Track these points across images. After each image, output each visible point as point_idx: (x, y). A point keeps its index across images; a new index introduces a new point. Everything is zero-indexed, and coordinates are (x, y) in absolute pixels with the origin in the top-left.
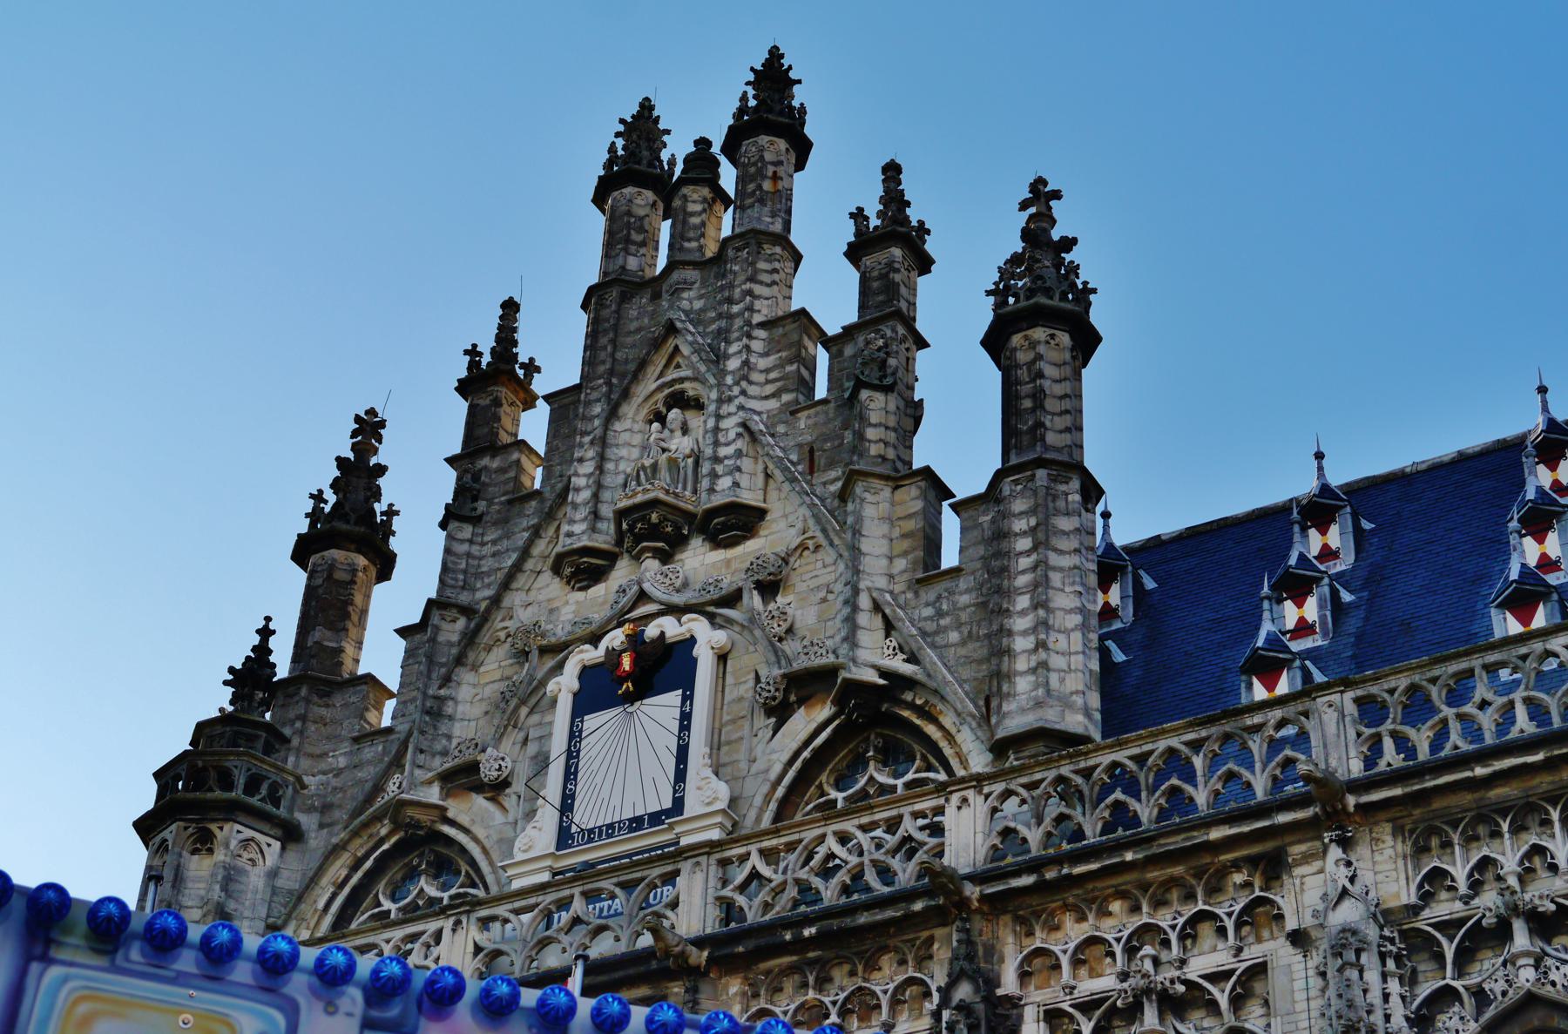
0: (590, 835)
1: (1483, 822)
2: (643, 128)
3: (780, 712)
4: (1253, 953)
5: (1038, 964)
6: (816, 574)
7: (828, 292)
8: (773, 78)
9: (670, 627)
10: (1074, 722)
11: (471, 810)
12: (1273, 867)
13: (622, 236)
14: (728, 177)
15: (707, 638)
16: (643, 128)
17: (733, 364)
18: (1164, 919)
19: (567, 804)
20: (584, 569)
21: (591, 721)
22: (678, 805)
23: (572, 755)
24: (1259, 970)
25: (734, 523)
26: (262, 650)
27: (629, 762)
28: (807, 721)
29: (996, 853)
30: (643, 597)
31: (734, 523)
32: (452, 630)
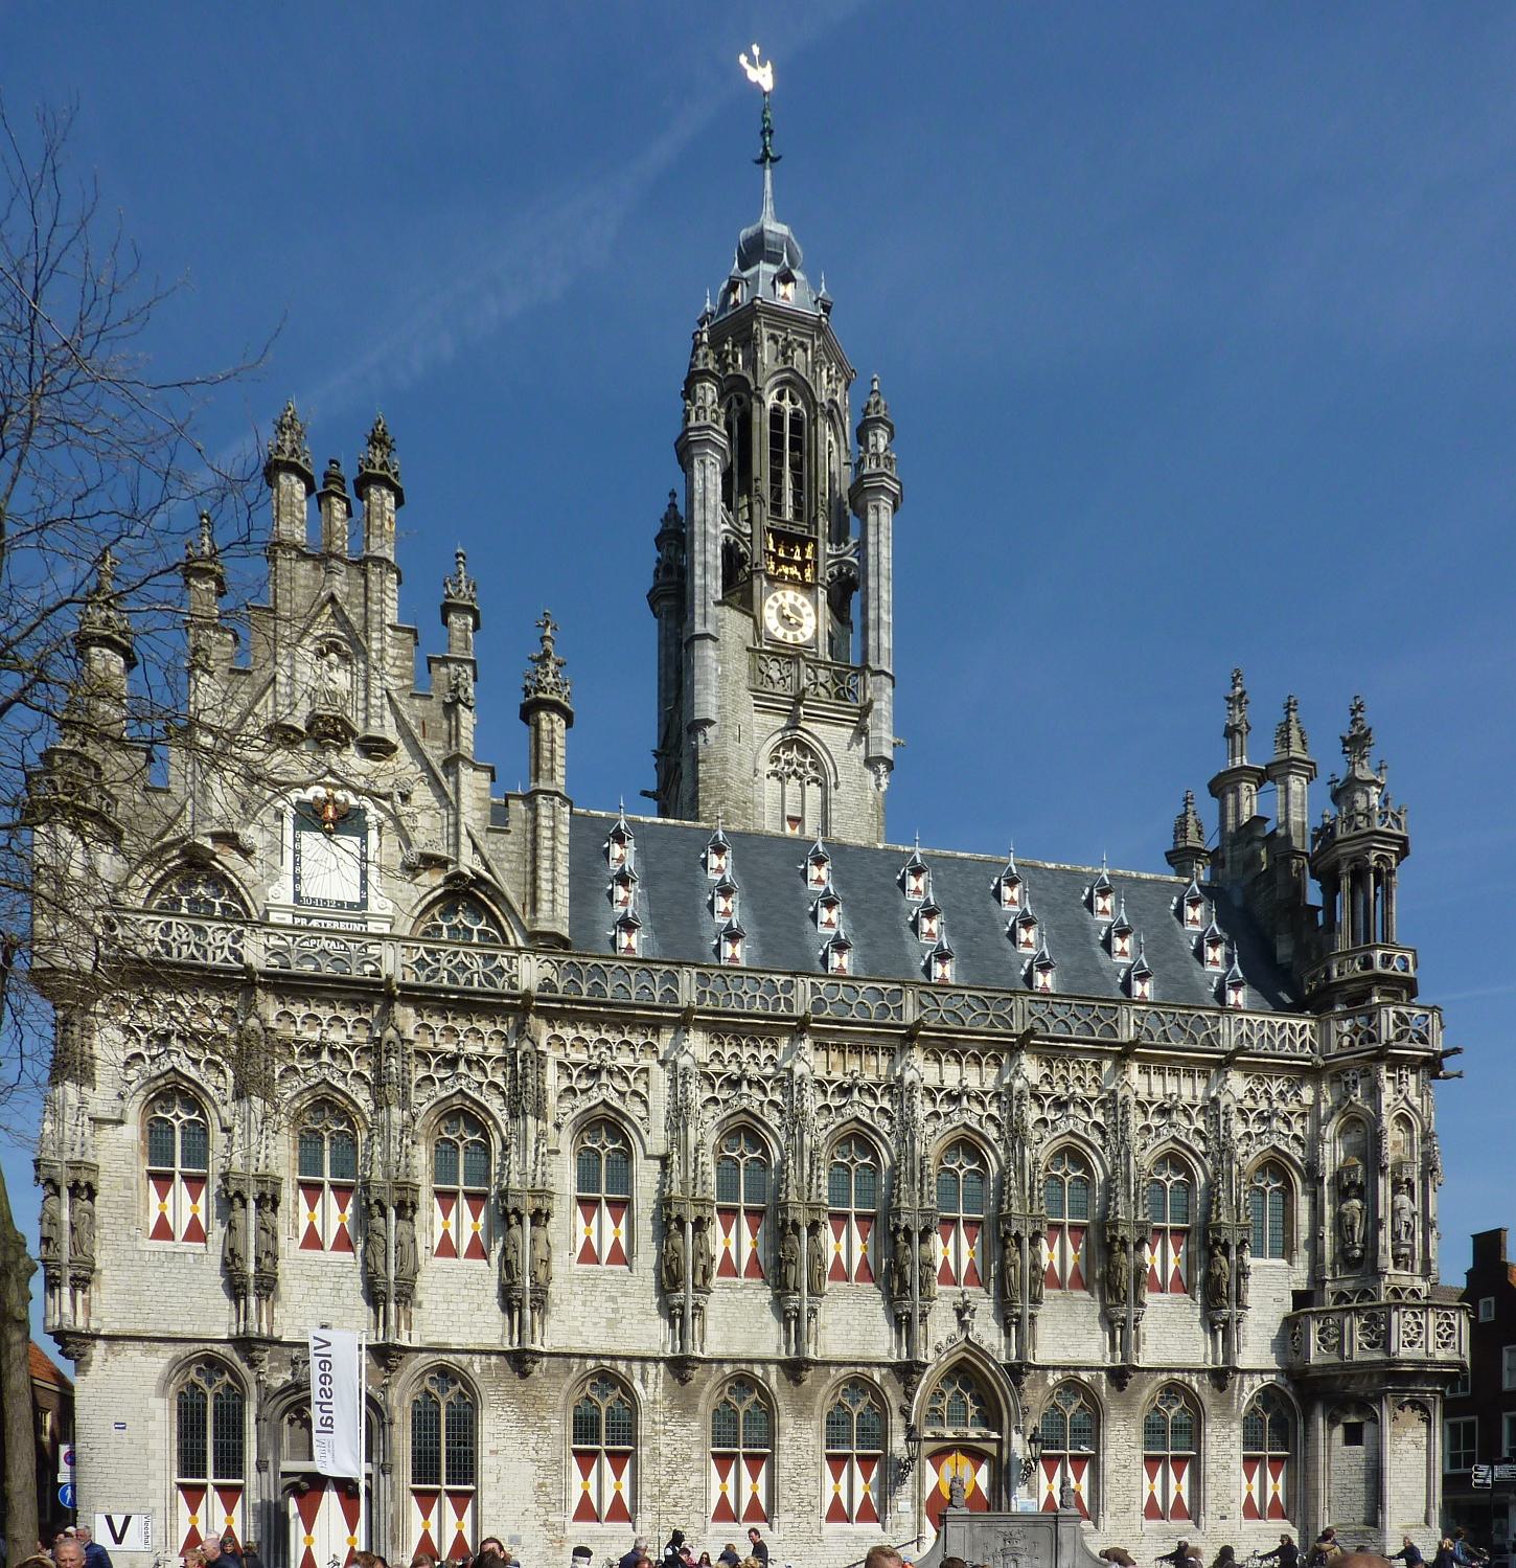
4: (643, 1063)
10: (565, 932)
12: (655, 1026)
24: (646, 1070)
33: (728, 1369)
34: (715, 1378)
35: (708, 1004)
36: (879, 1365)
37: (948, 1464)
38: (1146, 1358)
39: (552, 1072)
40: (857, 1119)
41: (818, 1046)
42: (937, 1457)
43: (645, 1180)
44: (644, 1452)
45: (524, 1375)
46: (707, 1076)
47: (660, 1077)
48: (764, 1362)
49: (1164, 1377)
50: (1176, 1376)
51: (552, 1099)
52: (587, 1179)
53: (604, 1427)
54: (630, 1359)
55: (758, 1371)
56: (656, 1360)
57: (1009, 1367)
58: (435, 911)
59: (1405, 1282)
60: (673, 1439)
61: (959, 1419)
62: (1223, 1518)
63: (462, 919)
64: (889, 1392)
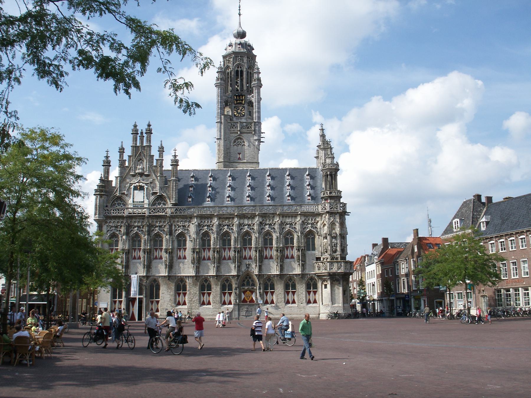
2: (135, 126)
5: (174, 221)
8: (149, 125)
9: (143, 185)
10: (177, 202)
12: (191, 218)
13: (135, 140)
14: (145, 135)
15: (146, 187)
16: (135, 126)
19: (133, 198)
21: (135, 191)
22: (143, 202)
23: (134, 194)
25: (148, 176)
27: (139, 196)
31: (148, 176)
34: (201, 279)
35: (200, 213)
37: (247, 293)
39: (173, 227)
41: (220, 218)
42: (244, 292)
43: (189, 245)
44: (188, 292)
51: (173, 231)
52: (179, 245)
61: (248, 284)
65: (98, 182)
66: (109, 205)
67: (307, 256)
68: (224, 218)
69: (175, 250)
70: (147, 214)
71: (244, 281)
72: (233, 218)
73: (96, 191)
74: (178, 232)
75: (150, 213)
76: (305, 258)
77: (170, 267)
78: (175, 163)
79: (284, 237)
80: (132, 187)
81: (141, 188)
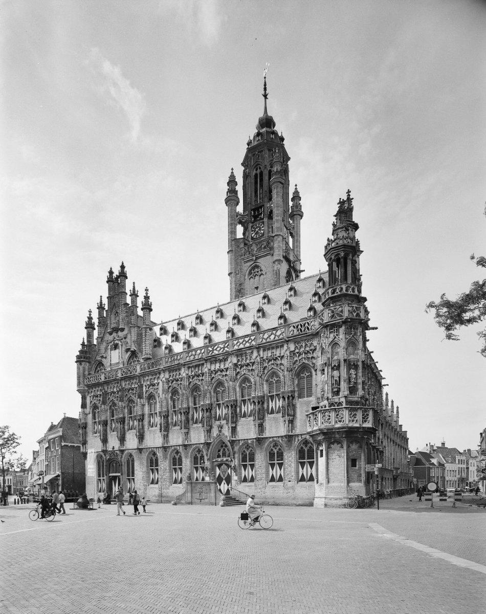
0: (114, 364)
1: (173, 371)
3: (127, 352)
5: (144, 381)
6: (129, 336)
7: (129, 300)
10: (148, 356)
11: (104, 360)
15: (120, 343)
17: (120, 309)
18: (153, 377)
20: (111, 334)
21: (112, 352)
25: (122, 330)
26: (84, 341)
28: (129, 353)
29: (141, 371)
30: (115, 338)
32: (100, 340)
33: (173, 448)
34: (171, 450)
36: (201, 444)
38: (267, 434)
39: (144, 387)
40: (196, 383)
41: (189, 368)
45: (141, 453)
46: (169, 381)
47: (161, 384)
48: (179, 446)
49: (271, 440)
50: (275, 439)
51: (144, 394)
53: (153, 463)
54: (156, 448)
55: (178, 448)
56: (161, 447)
57: (229, 441)
58: (131, 359)
59: (337, 400)
60: (164, 465)
61: (224, 455)
62: (290, 481)
63: (135, 359)
64: (204, 450)
65: (80, 348)
66: (92, 372)
67: (298, 406)
68: (192, 367)
69: (146, 417)
70: (119, 375)
71: (219, 451)
72: (203, 364)
73: (78, 357)
74: (148, 393)
75: (123, 375)
76: (294, 410)
77: (141, 437)
78: (147, 307)
79: (267, 381)
80: (109, 347)
81: (116, 347)
